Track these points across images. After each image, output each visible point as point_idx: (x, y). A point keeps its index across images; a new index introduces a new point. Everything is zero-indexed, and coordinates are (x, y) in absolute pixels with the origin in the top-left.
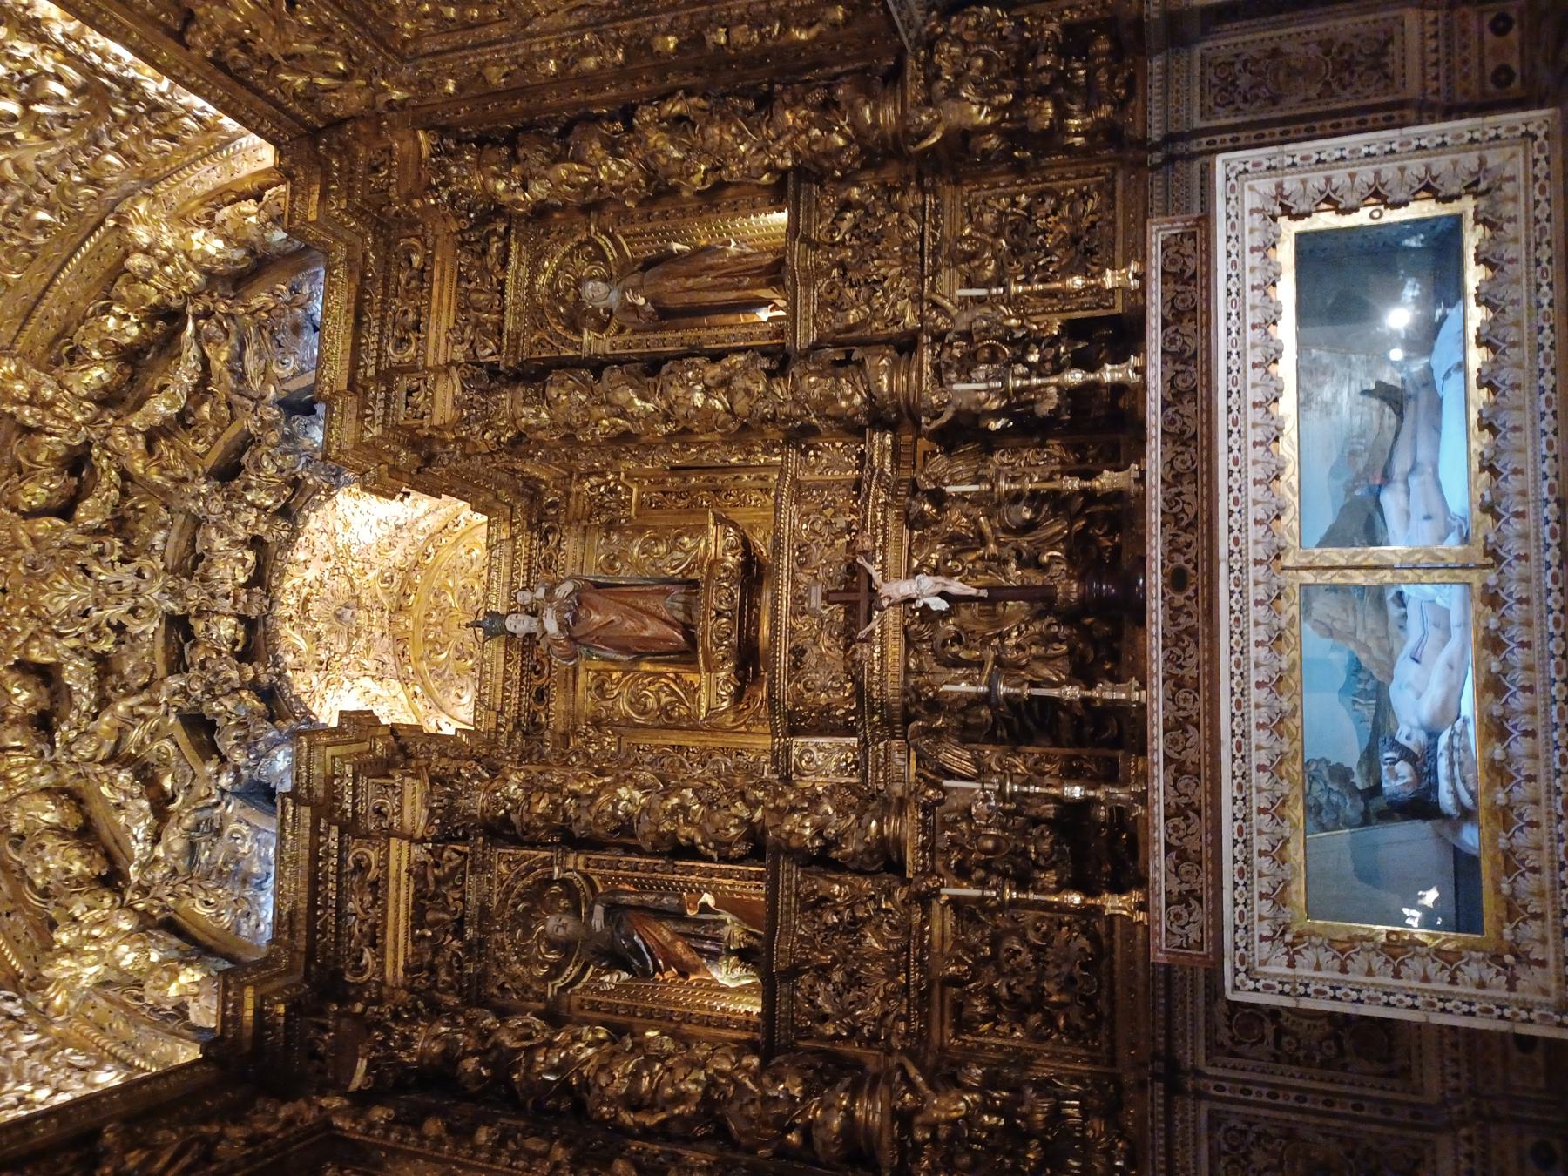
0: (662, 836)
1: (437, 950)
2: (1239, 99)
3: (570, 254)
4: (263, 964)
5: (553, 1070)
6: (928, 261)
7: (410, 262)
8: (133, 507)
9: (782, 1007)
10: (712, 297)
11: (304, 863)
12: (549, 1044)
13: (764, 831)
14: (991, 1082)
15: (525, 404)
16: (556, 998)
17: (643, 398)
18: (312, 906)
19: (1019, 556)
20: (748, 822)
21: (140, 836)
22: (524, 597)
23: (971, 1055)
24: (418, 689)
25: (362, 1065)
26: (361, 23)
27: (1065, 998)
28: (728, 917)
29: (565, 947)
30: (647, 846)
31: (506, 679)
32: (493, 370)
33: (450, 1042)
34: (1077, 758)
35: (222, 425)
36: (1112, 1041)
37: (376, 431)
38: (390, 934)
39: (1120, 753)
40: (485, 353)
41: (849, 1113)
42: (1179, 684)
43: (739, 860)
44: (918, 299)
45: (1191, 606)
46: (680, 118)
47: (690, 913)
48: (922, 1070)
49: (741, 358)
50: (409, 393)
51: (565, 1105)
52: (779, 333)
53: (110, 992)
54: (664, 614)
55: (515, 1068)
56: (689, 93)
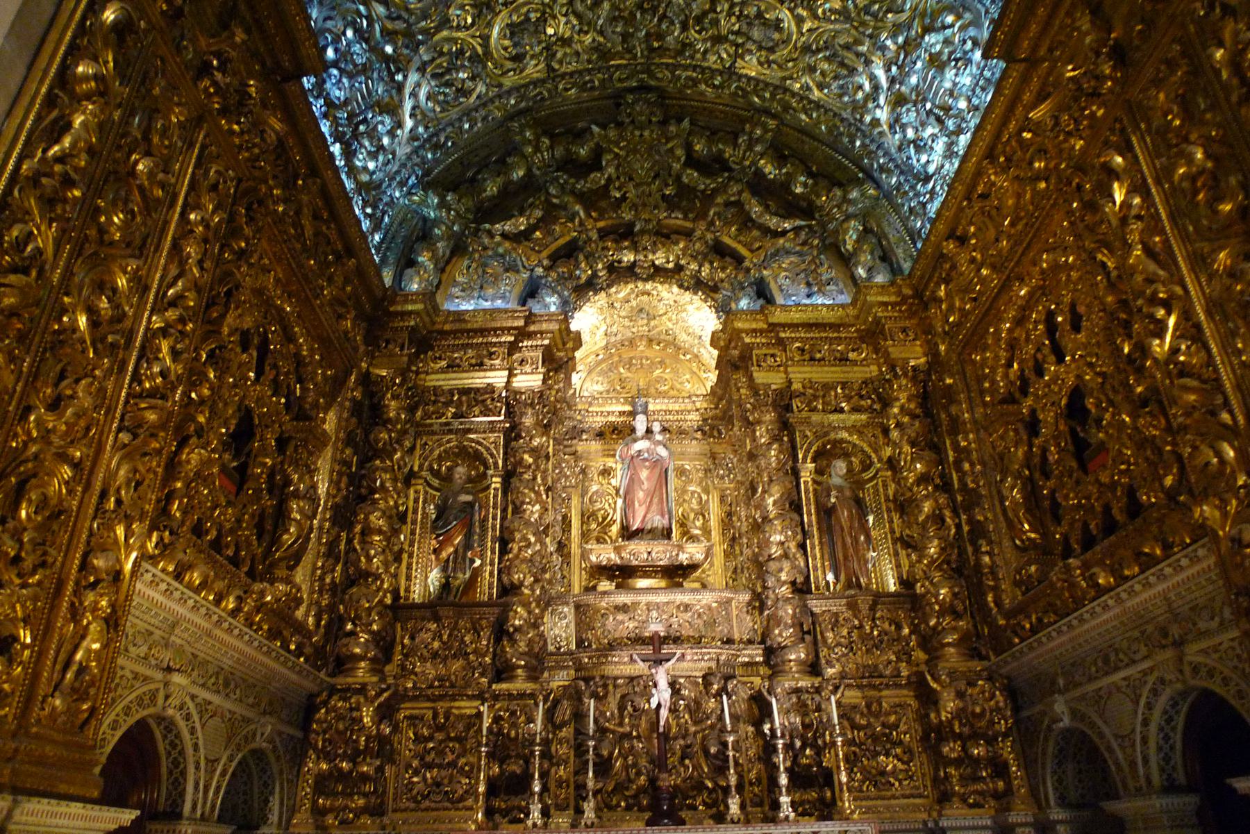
0: (512, 533)
1: (449, 403)
3: (863, 451)
4: (436, 308)
5: (382, 484)
6: (865, 682)
7: (853, 350)
8: (697, 197)
9: (417, 613)
10: (839, 544)
11: (494, 325)
12: (395, 480)
13: (516, 594)
14: (382, 740)
15: (767, 430)
17: (775, 503)
18: (468, 331)
19: (688, 746)
20: (521, 584)
21: (507, 228)
22: (656, 427)
23: (396, 729)
24: (601, 357)
26: (973, 334)
27: (430, 781)
28: (467, 576)
29: (447, 478)
31: (608, 413)
32: (788, 408)
33: (398, 419)
34: (568, 786)
36: (405, 810)
37: (747, 340)
38: (454, 375)
39: (572, 812)
40: (796, 403)
41: (362, 658)
43: (499, 579)
44: (843, 676)
46: (943, 521)
47: (469, 554)
48: (387, 700)
49: (802, 564)
50: (773, 355)
54: (649, 516)
55: (383, 461)
56: (959, 527)
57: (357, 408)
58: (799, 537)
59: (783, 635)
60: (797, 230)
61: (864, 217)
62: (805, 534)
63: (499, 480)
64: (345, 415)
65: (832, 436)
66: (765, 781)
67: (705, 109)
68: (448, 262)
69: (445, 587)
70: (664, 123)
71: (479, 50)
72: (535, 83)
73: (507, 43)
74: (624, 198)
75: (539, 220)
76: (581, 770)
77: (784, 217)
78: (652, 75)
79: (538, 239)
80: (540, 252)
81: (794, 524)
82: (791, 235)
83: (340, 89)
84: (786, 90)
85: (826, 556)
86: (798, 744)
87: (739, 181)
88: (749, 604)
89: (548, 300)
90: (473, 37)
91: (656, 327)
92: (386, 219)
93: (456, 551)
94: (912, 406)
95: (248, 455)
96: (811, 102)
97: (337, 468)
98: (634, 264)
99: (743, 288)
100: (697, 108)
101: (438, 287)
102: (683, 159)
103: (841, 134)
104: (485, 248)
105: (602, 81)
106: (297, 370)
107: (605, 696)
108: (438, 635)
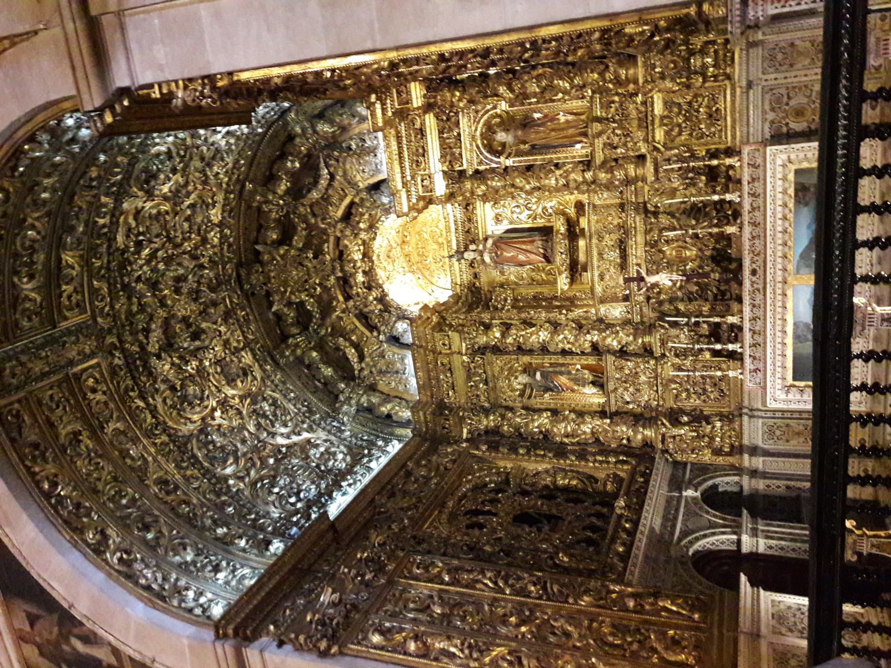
2: (777, 64)
5: (537, 428)
6: (650, 128)
17: (529, 183)
18: (430, 379)
20: (592, 342)
21: (355, 360)
25: (465, 430)
28: (586, 372)
30: (551, 350)
35: (342, 199)
42: (754, 306)
44: (646, 140)
45: (758, 281)
50: (422, 181)
51: (541, 437)
52: (587, 156)
53: (361, 414)
54: (534, 251)
56: (543, 65)
57: (494, 447)
60: (327, 166)
62: (550, 161)
64: (500, 455)
67: (244, 234)
68: (382, 393)
69: (593, 383)
71: (248, 401)
72: (254, 355)
73: (239, 384)
74: (320, 285)
75: (345, 340)
77: (317, 169)
78: (230, 276)
79: (358, 339)
80: (367, 337)
82: (332, 170)
83: (310, 489)
84: (228, 184)
86: (691, 175)
87: (296, 208)
89: (400, 330)
90: (243, 406)
91: (396, 242)
92: (365, 438)
94: (458, 94)
95: (539, 514)
96: (234, 167)
97: (533, 458)
98: (364, 272)
99: (375, 201)
100: (244, 239)
101: (401, 398)
102: (286, 248)
103: (253, 142)
104: (371, 372)
105: (243, 309)
106: (480, 488)
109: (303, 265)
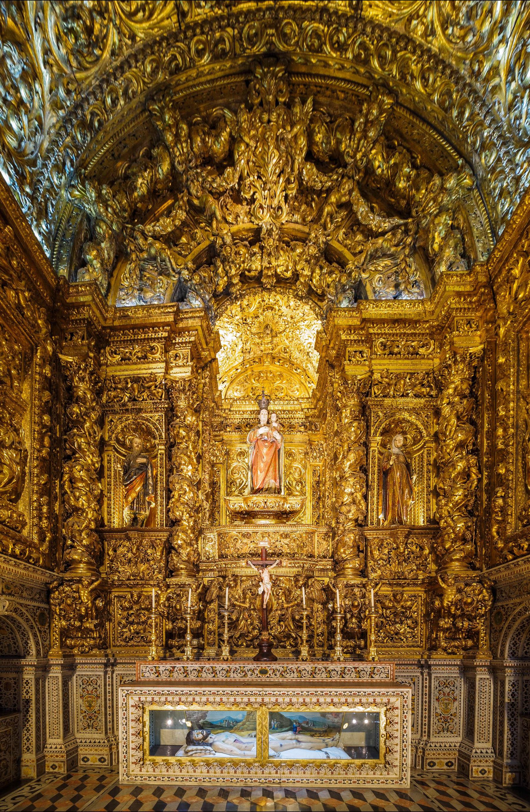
16: (110, 445)
21: (157, 228)
36: (120, 646)
58: (364, 490)
59: (345, 553)
61: (454, 212)
63: (163, 447)
65: (397, 416)
66: (326, 634)
70: (289, 106)
76: (221, 626)
81: (362, 480)
82: (389, 236)
85: (380, 503)
88: (326, 534)
93: (138, 496)
107: (236, 585)
108: (130, 550)
109: (279, 176)
